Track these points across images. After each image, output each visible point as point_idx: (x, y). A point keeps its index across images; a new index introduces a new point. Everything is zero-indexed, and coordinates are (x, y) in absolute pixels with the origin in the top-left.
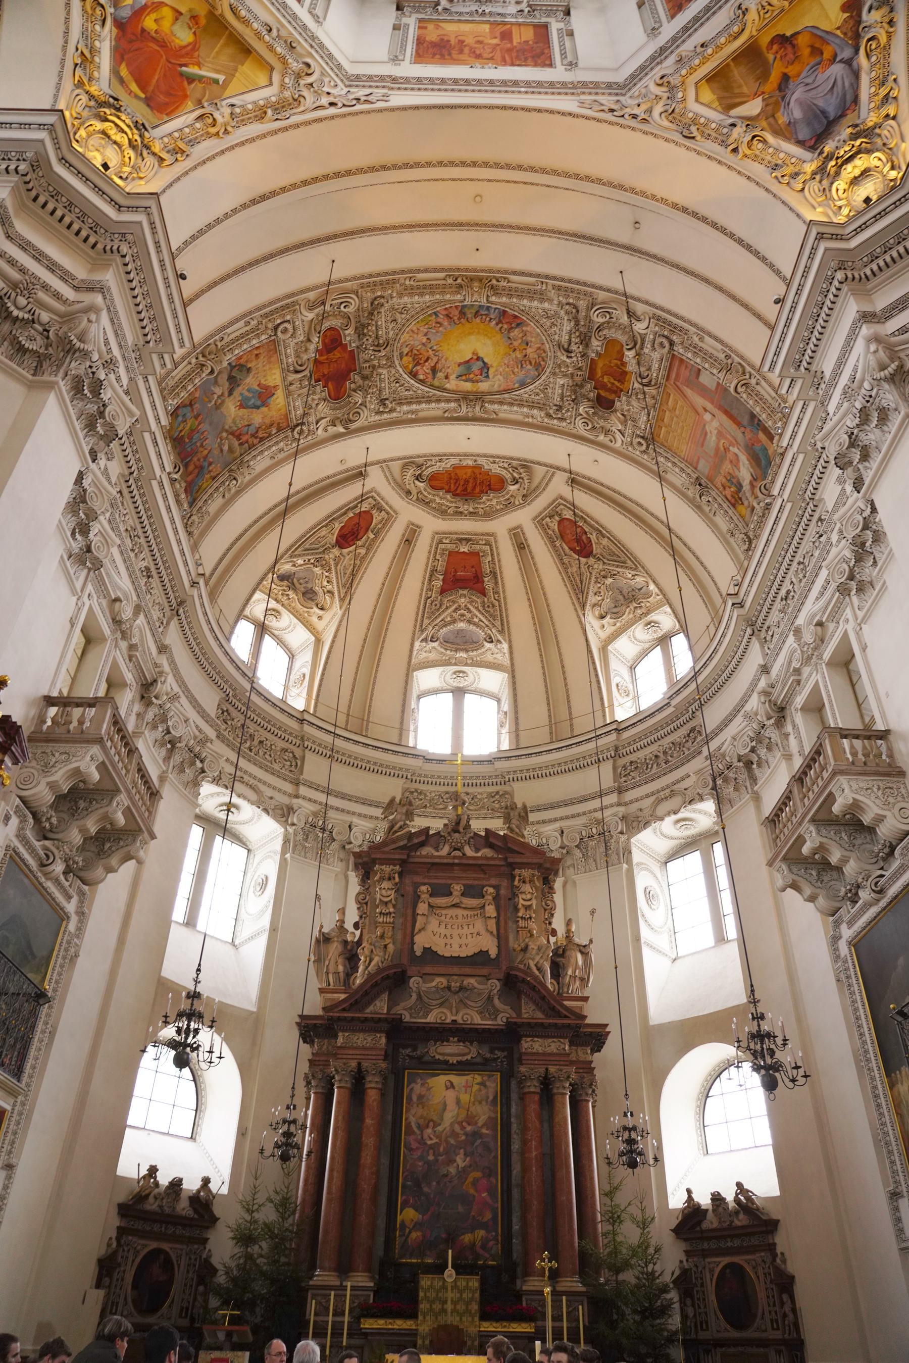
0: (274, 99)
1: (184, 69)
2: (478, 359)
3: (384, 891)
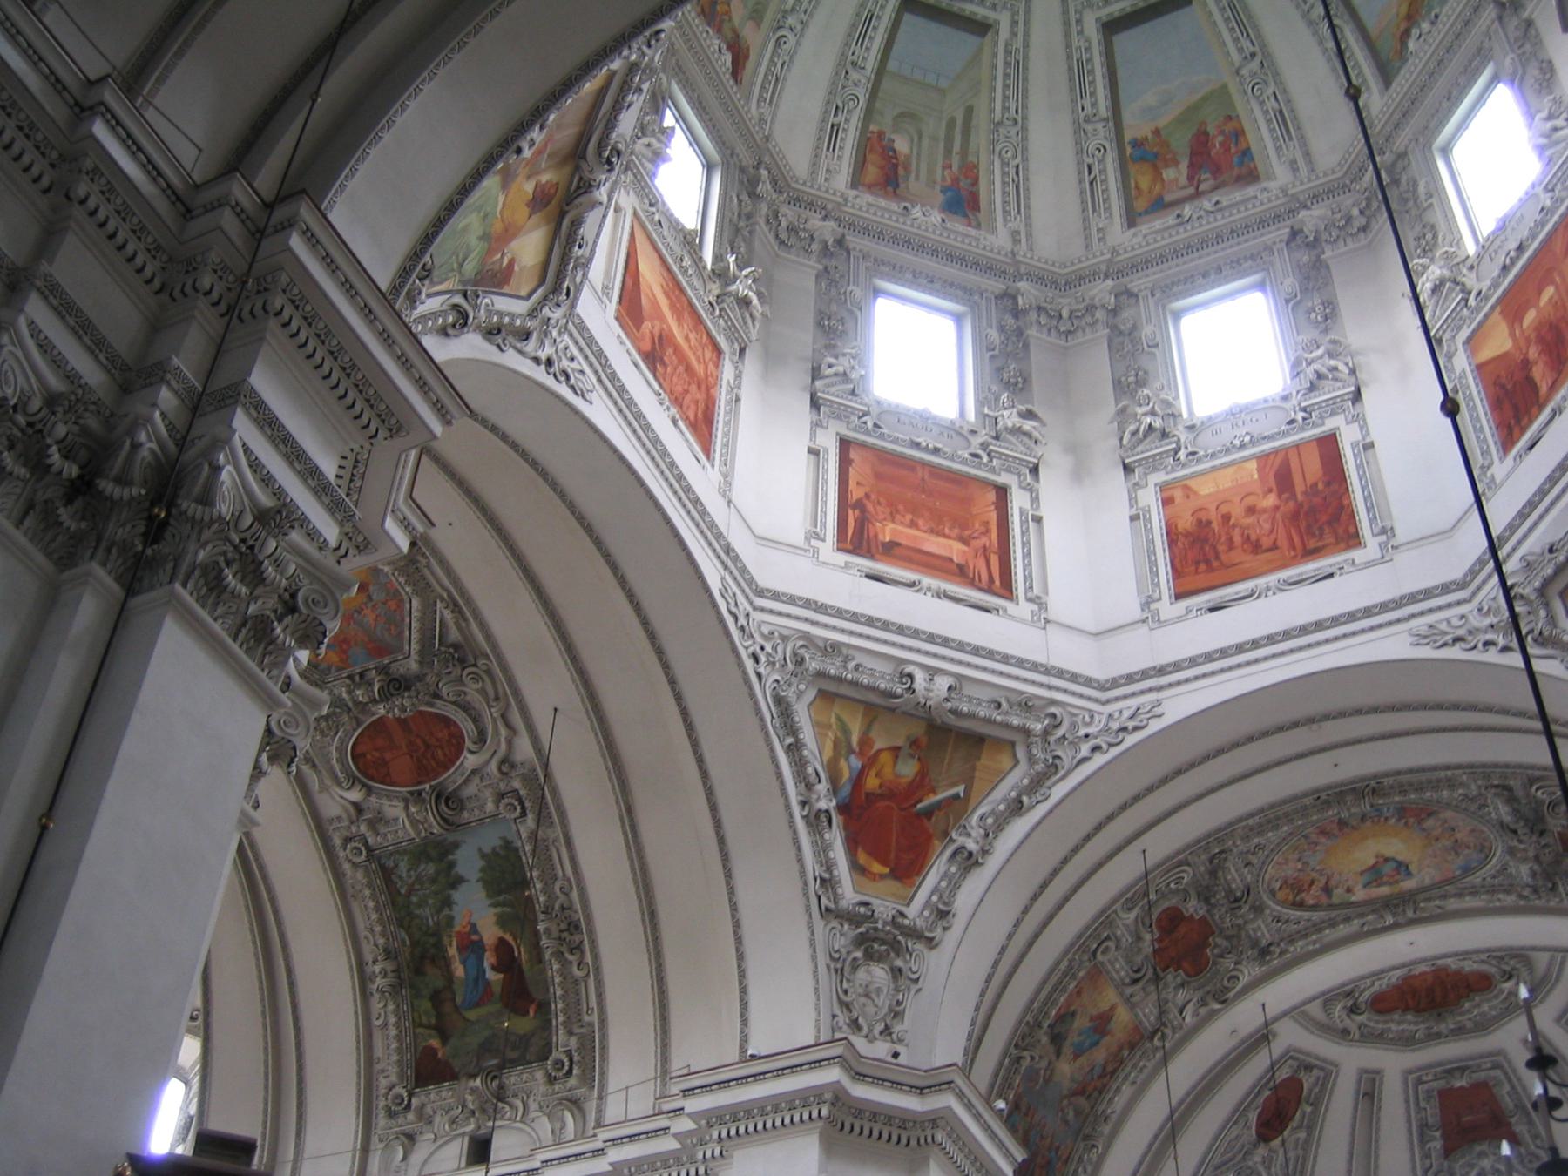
0: (1026, 781)
1: (919, 806)
2: (1387, 860)
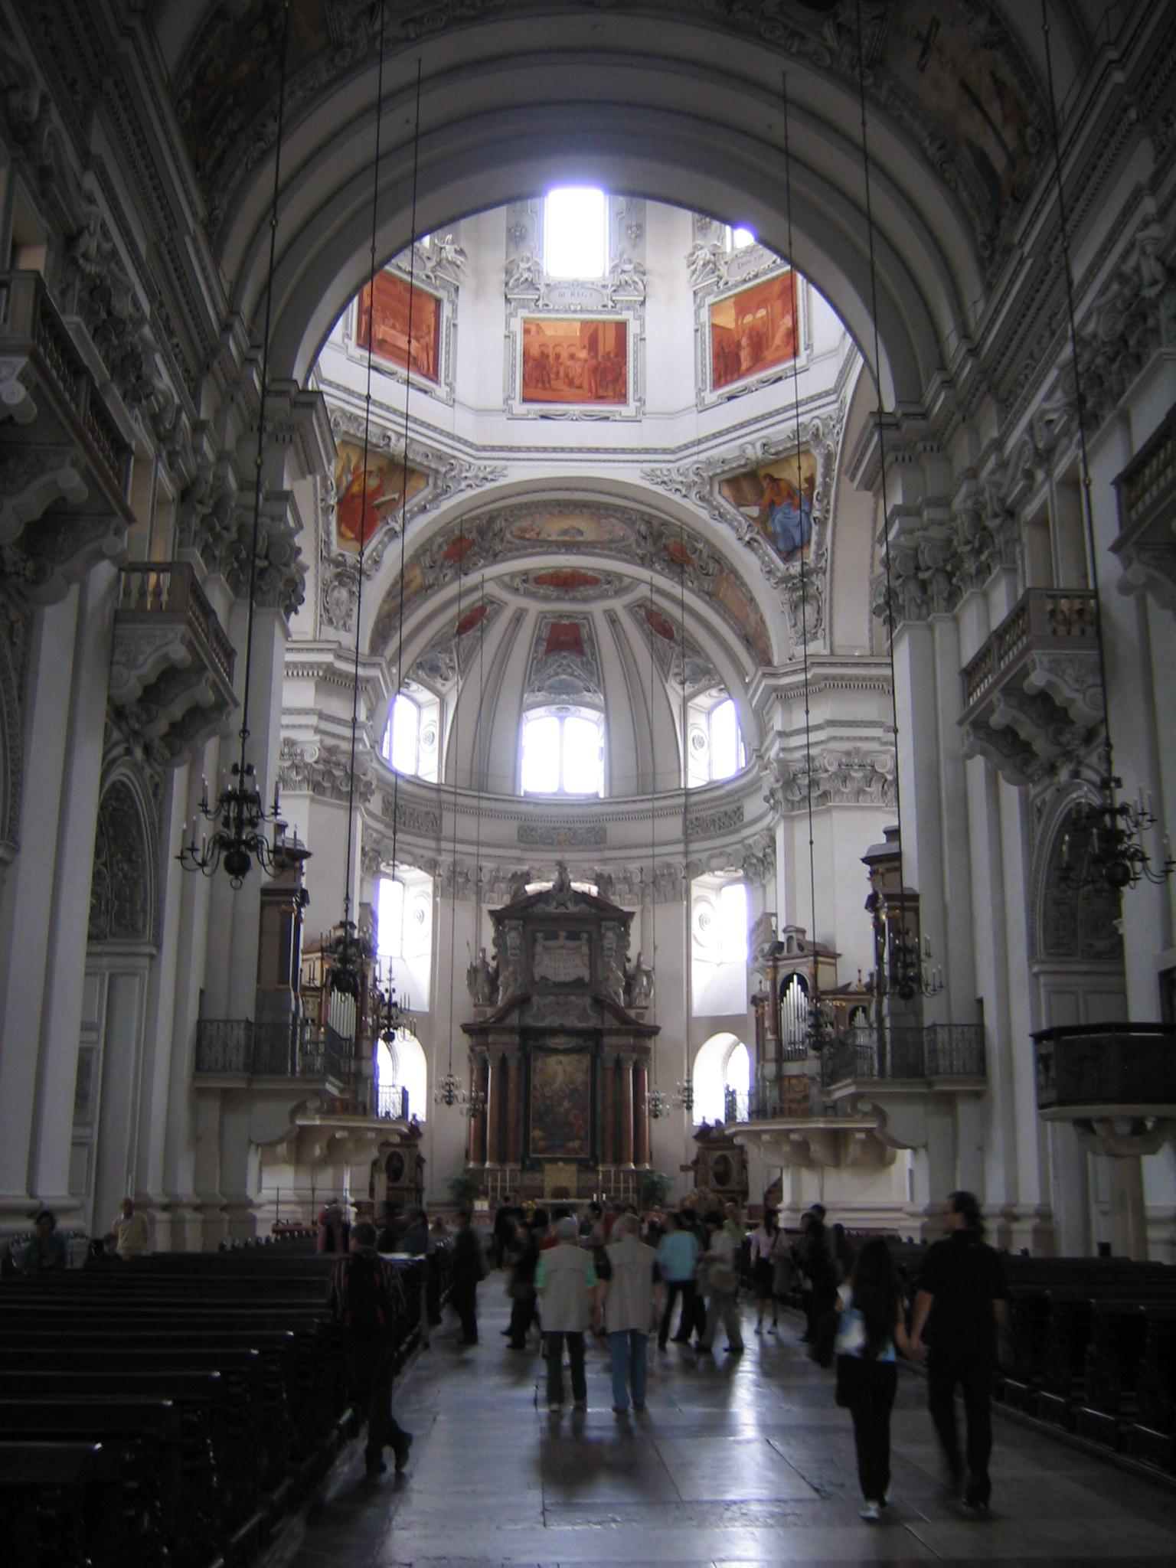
3: (513, 938)
